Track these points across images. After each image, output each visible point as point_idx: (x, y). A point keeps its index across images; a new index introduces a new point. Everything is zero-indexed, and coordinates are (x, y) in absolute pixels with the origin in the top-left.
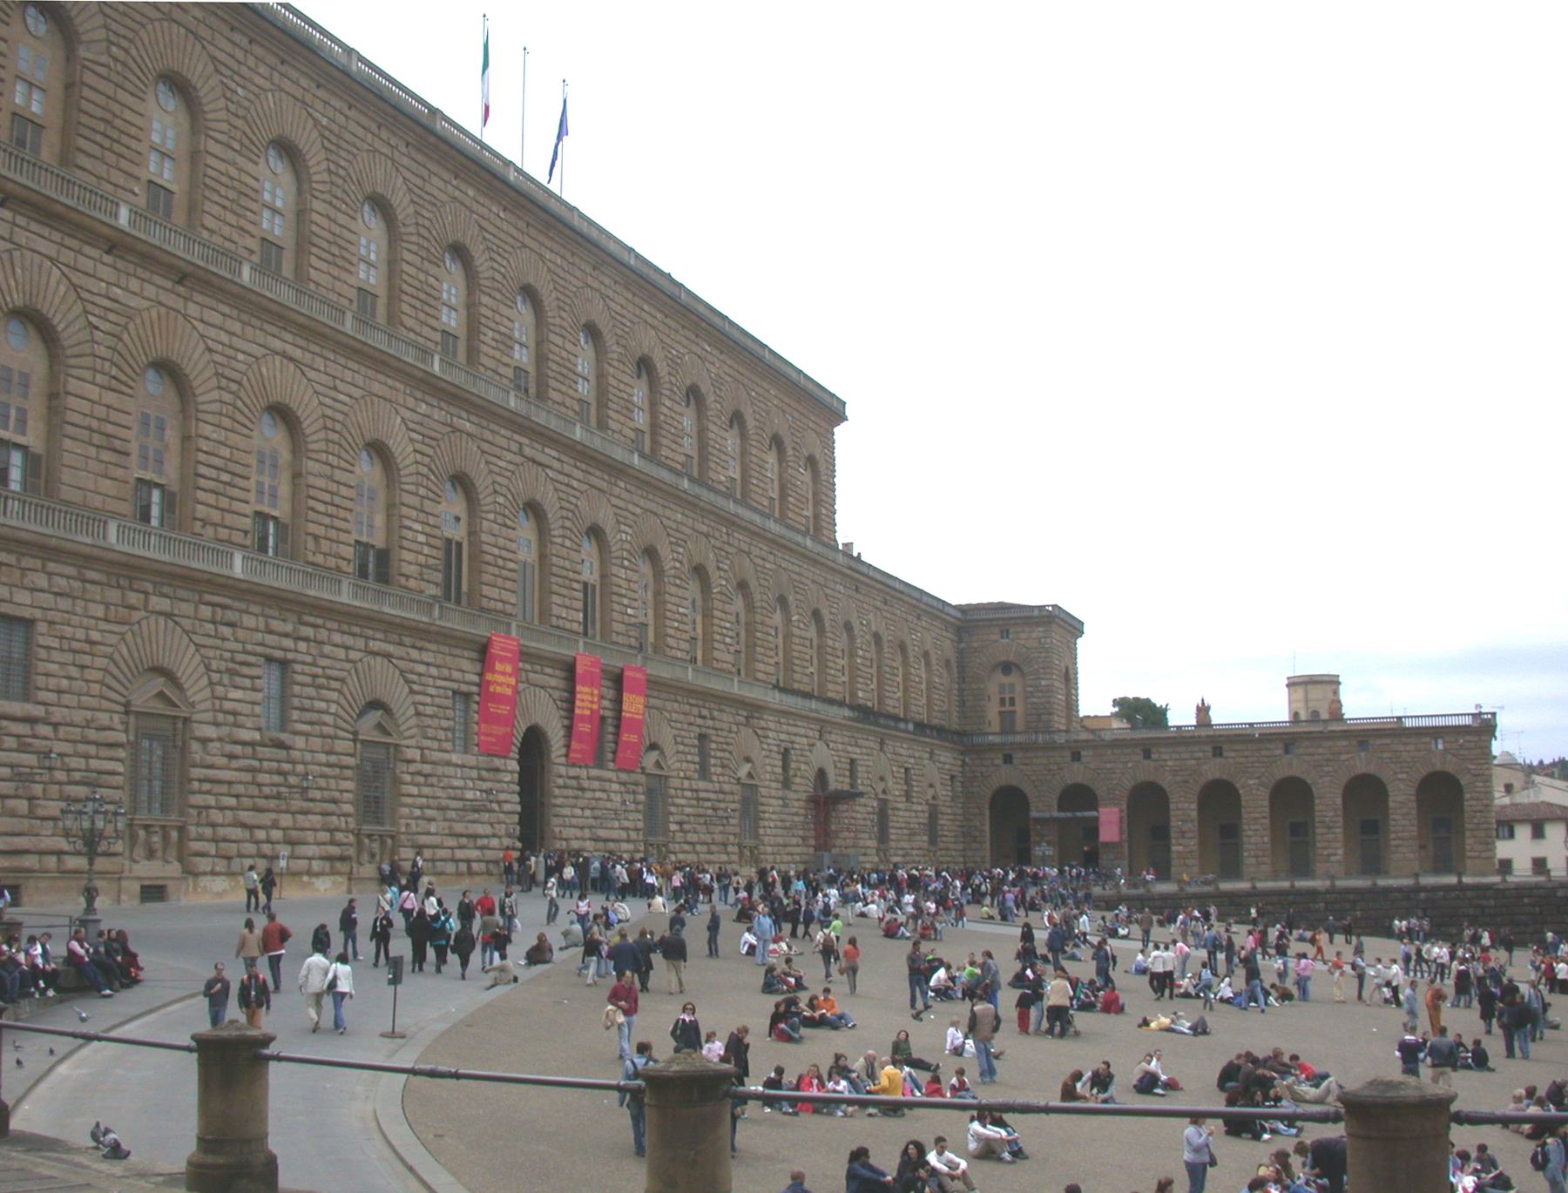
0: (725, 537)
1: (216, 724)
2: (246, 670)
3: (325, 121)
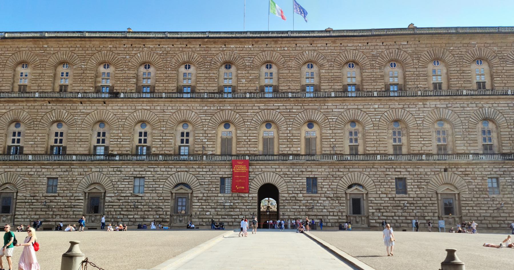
0: (422, 106)
1: (114, 193)
2: (125, 180)
3: (161, 52)
